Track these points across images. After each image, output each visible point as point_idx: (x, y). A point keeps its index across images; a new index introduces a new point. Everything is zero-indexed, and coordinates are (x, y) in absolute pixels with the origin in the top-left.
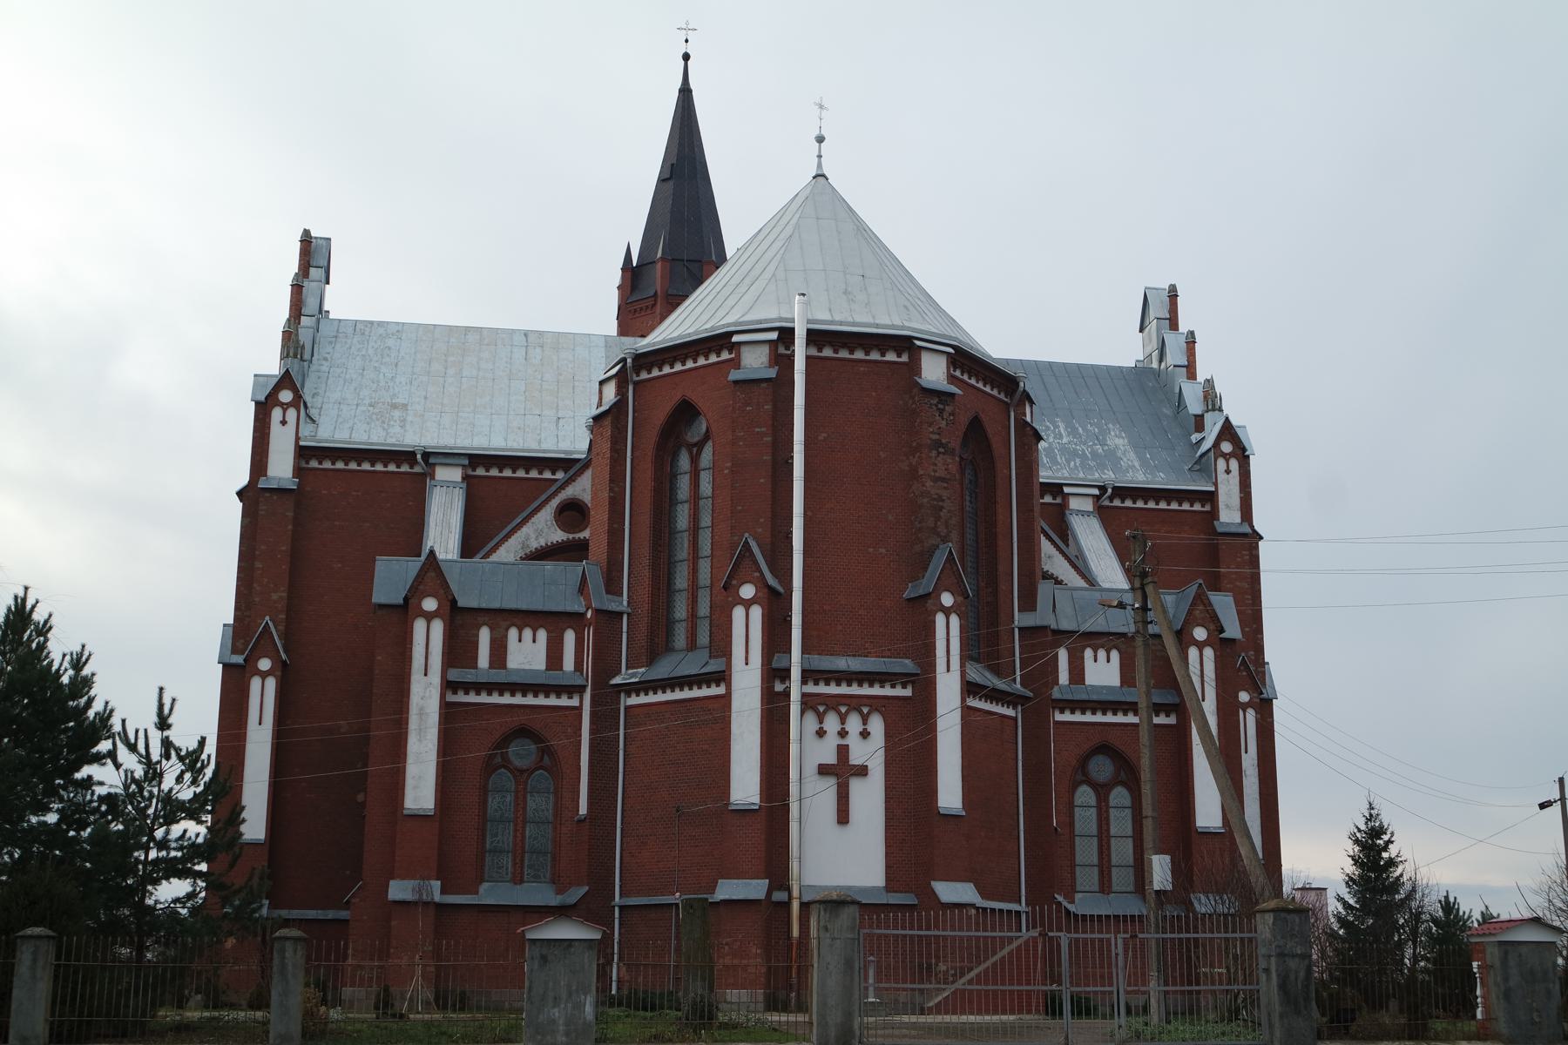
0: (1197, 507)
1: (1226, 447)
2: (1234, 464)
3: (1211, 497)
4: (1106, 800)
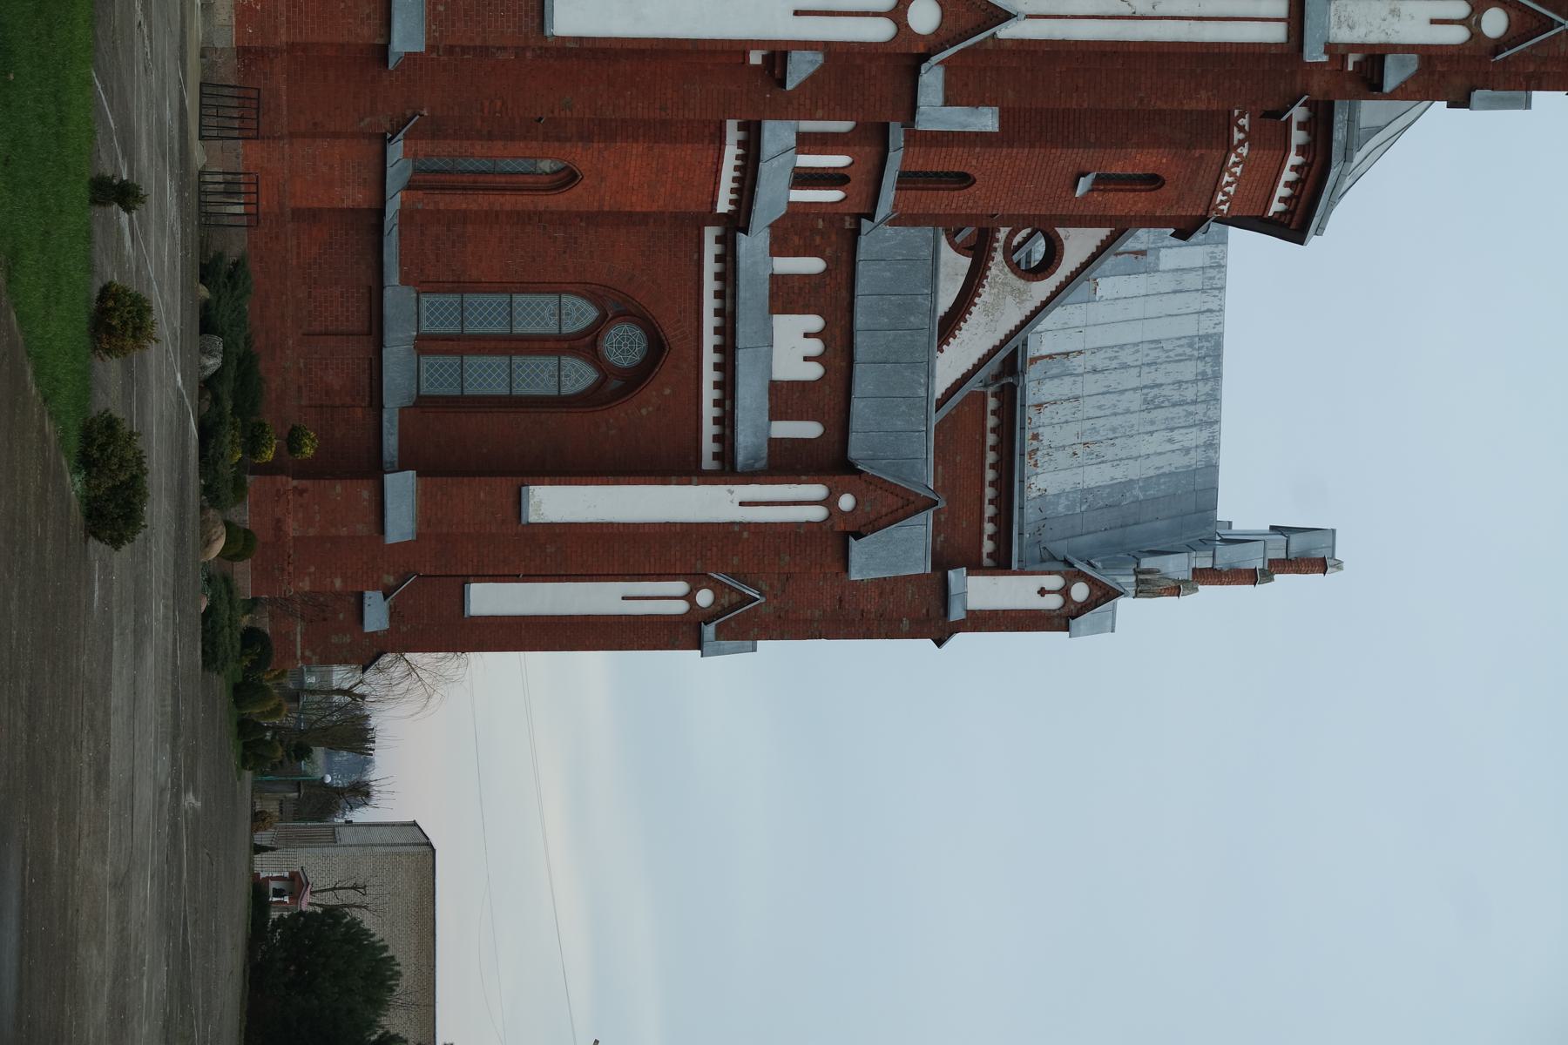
0: (988, 546)
1: (1080, 592)
2: (1053, 602)
3: (1002, 564)
4: (574, 352)
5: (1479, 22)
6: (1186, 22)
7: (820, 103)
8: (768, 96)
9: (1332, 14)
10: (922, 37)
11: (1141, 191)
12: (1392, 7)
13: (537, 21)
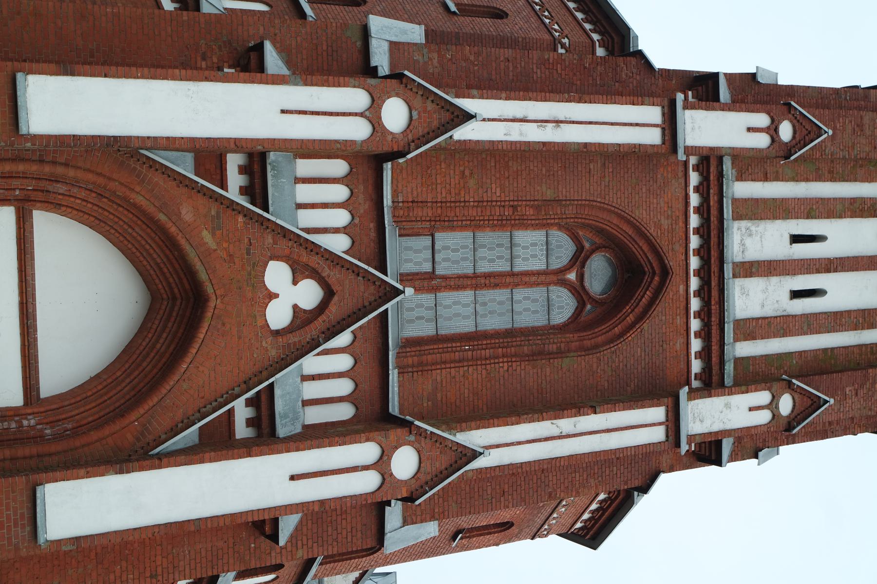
5: (777, 407)
6: (598, 435)
7: (300, 543)
8: (253, 545)
9: (689, 412)
10: (405, 482)
11: (495, 533)
12: (726, 402)
13: (28, 529)
